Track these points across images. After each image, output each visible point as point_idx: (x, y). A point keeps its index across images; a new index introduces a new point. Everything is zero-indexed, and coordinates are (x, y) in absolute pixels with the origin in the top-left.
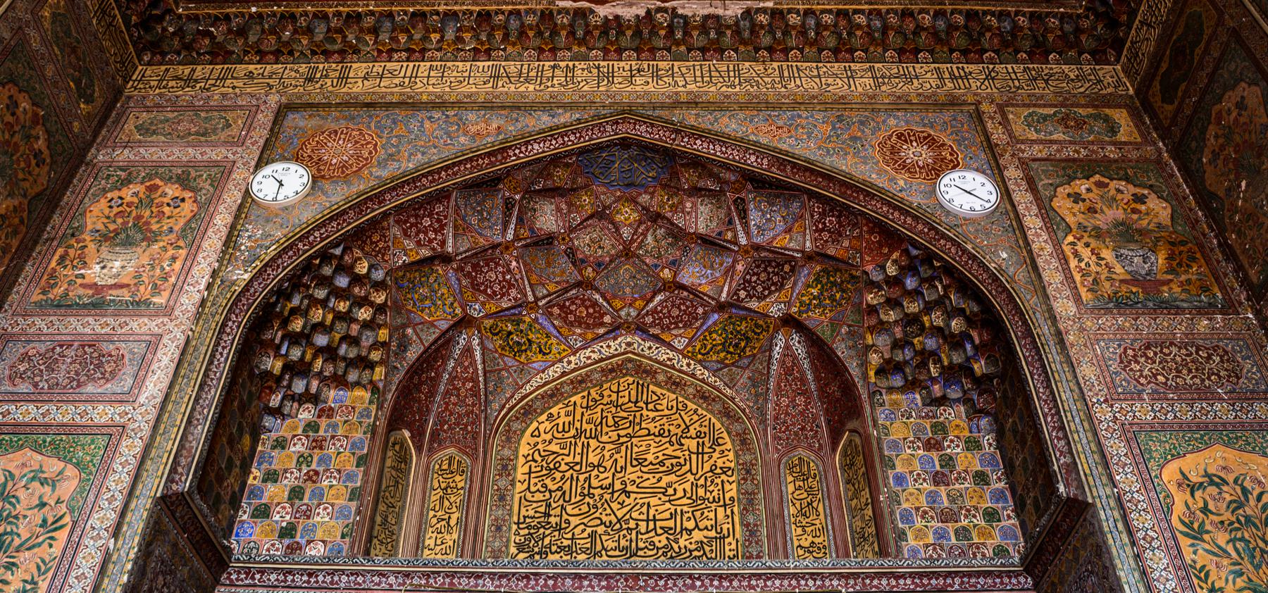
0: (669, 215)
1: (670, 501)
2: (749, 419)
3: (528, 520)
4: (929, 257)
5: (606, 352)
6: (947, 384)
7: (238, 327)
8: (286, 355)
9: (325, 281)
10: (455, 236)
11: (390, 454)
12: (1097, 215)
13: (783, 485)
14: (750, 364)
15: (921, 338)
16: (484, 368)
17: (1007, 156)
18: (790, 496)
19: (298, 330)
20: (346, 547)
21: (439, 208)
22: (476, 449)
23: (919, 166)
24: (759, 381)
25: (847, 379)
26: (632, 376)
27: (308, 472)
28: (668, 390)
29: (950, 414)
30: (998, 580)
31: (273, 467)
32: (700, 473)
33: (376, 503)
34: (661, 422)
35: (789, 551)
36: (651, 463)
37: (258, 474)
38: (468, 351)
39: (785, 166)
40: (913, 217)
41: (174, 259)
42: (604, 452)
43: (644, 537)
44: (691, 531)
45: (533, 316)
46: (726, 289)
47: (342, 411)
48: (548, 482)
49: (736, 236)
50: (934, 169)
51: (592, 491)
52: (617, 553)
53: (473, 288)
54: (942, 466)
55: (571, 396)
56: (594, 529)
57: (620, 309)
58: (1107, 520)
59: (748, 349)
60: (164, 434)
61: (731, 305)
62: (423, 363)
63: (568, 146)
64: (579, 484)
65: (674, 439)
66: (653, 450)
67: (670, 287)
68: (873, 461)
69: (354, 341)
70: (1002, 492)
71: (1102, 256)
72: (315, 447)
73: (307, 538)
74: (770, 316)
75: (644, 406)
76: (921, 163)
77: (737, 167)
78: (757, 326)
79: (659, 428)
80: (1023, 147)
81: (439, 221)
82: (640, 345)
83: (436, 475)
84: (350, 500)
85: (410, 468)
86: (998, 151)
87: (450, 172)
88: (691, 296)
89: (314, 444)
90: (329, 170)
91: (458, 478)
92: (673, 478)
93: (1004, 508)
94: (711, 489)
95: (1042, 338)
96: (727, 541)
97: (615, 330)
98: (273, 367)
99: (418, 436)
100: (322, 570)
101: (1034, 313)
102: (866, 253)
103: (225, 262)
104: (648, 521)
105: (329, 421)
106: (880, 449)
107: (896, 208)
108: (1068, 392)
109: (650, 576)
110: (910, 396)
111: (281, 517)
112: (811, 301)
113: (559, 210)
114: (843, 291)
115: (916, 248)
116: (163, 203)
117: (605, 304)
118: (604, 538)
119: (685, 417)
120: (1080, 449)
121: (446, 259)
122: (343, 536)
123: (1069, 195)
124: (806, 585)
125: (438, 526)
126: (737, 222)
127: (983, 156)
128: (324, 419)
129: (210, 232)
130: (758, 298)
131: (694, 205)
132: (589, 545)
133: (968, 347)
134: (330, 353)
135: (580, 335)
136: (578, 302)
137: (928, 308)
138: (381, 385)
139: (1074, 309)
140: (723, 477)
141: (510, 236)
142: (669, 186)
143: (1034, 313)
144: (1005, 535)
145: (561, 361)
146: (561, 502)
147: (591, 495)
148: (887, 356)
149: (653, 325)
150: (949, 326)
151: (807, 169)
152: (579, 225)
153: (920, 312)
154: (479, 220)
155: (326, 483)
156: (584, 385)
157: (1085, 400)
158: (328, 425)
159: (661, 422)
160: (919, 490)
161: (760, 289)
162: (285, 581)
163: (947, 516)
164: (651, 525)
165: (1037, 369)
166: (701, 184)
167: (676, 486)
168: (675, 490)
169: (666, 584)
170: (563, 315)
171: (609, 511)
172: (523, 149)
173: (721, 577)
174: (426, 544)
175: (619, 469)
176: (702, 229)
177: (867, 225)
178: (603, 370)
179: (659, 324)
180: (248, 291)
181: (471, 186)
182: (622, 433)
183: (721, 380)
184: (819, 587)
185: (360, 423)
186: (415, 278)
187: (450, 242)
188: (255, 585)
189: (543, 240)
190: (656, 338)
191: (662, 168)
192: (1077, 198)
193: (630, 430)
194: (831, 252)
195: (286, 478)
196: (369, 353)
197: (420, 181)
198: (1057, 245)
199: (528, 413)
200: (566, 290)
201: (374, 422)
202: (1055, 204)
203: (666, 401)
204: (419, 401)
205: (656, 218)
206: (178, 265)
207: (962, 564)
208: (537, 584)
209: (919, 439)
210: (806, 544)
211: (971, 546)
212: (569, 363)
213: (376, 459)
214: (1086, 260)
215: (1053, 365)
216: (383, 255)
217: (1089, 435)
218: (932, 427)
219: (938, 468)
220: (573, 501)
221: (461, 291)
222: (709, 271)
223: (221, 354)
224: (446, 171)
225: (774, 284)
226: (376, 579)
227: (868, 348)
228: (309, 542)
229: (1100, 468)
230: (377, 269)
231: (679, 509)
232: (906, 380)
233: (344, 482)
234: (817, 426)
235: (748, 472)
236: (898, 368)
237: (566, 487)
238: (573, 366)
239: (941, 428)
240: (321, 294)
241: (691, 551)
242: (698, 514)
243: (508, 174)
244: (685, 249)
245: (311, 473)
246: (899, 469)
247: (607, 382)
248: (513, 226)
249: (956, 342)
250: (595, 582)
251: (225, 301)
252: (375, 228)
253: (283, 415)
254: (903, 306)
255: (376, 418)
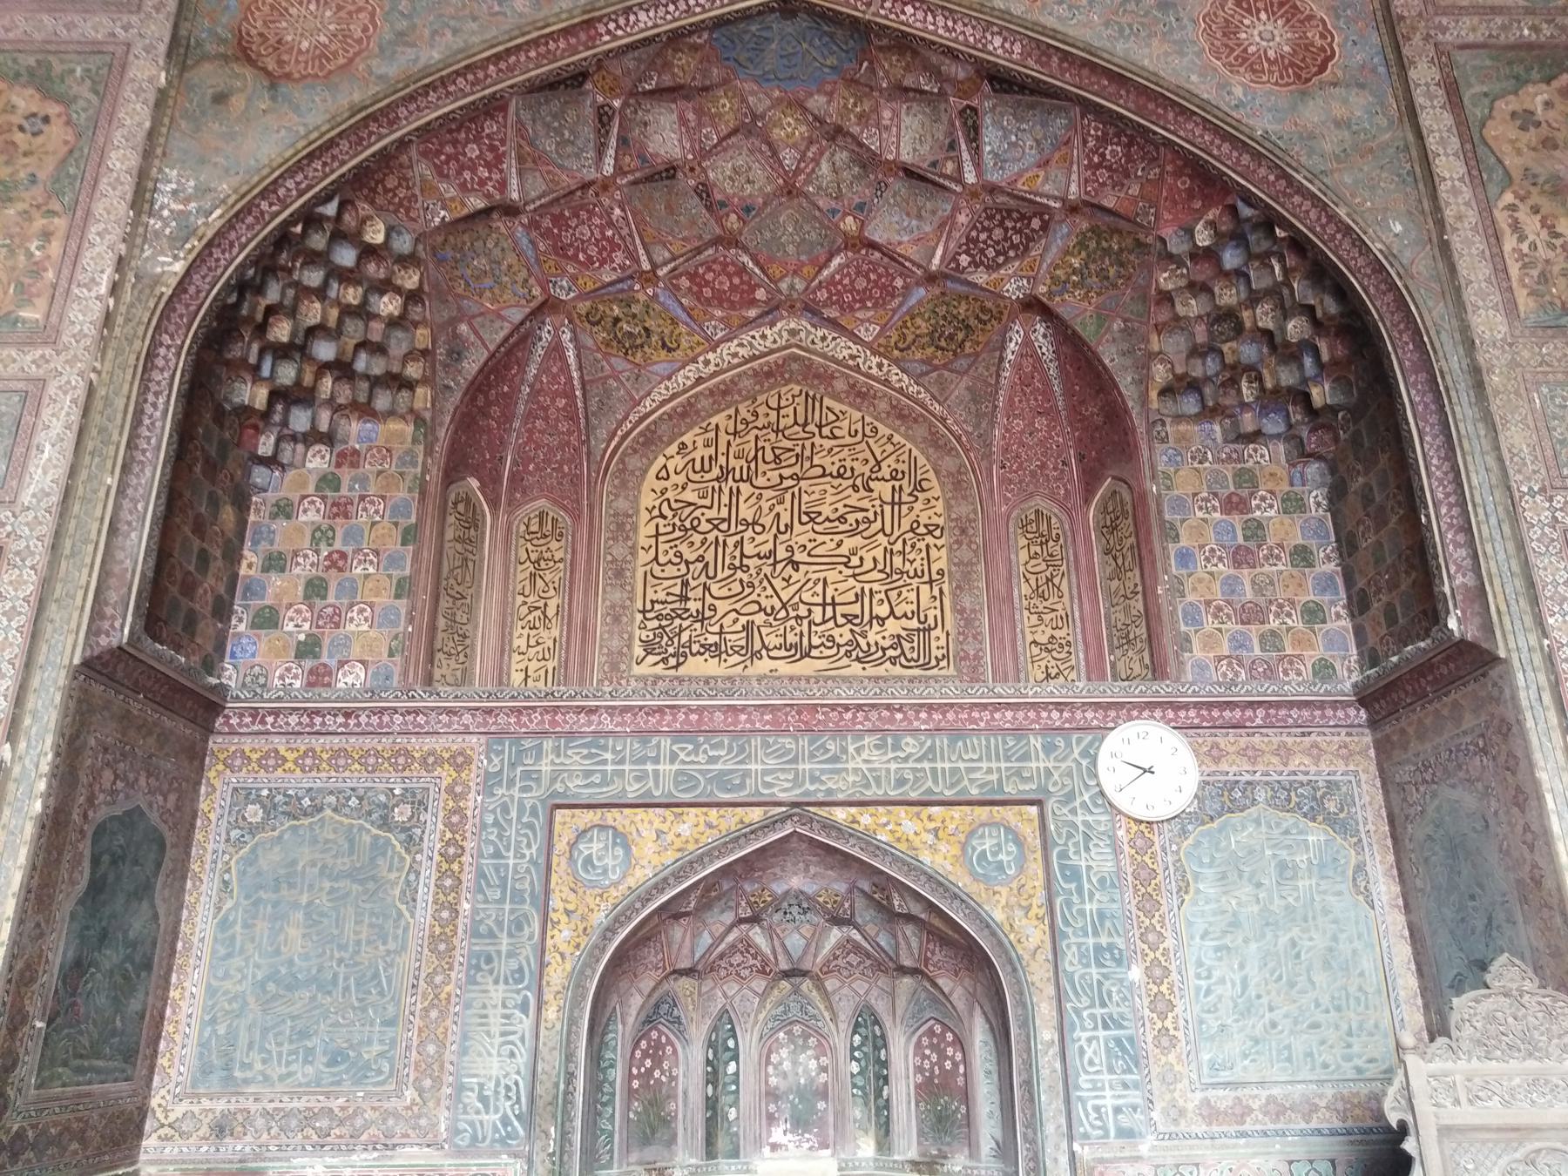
0: (855, 130)
1: (854, 576)
2: (966, 451)
3: (657, 607)
4: (1269, 222)
5: (760, 346)
6: (1264, 411)
7: (178, 355)
8: (272, 377)
9: (315, 258)
10: (520, 173)
11: (451, 519)
12: (1557, 153)
13: (1013, 550)
14: (970, 367)
15: (1234, 344)
16: (582, 377)
17: (1417, 39)
18: (1022, 569)
19: (285, 339)
20: (397, 671)
21: (490, 127)
22: (578, 501)
23: (1268, 60)
24: (982, 396)
25: (1115, 401)
26: (798, 383)
27: (330, 554)
28: (850, 405)
29: (1262, 456)
30: (1318, 713)
31: (275, 547)
32: (896, 534)
33: (436, 599)
34: (841, 456)
35: (1020, 649)
36: (827, 519)
37: (254, 559)
38: (556, 349)
39: (1049, 57)
40: (1252, 155)
41: (46, 235)
42: (762, 503)
43: (819, 629)
44: (883, 620)
45: (650, 291)
46: (939, 252)
47: (373, 456)
48: (683, 548)
49: (960, 169)
50: (1292, 64)
51: (745, 561)
52: (783, 653)
53: (557, 254)
54: (1246, 538)
55: (711, 416)
56: (750, 618)
57: (781, 278)
58: (1527, 687)
59: (968, 344)
60: (73, 555)
61: (946, 276)
62: (490, 373)
63: (695, 14)
64: (728, 551)
65: (859, 482)
66: (830, 499)
67: (854, 246)
68: (1149, 532)
69: (379, 349)
70: (1331, 578)
71: (1559, 229)
72: (336, 515)
73: (338, 657)
74: (1004, 297)
75: (816, 430)
76: (1271, 54)
77: (971, 56)
78: (983, 309)
79: (838, 464)
80: (1445, 21)
81: (492, 148)
82: (809, 333)
83: (522, 541)
84: (397, 596)
85: (484, 533)
86: (1402, 29)
87: (503, 65)
88: (886, 260)
89: (335, 510)
90: (297, 61)
91: (554, 545)
92: (857, 541)
93: (1332, 603)
94: (911, 557)
95: (1448, 377)
96: (934, 634)
97: (771, 311)
98: (253, 397)
99: (490, 483)
100: (364, 709)
101: (1438, 333)
102: (1166, 208)
103: (139, 241)
104: (824, 605)
105: (353, 472)
106: (1160, 512)
107: (1226, 137)
108: (1483, 472)
109: (833, 707)
110: (1207, 426)
111: (296, 626)
112: (1069, 276)
113: (683, 121)
114: (1122, 265)
115: (1251, 205)
116: (10, 124)
117: (757, 270)
118: (764, 631)
119: (874, 447)
120: (1494, 570)
121: (511, 211)
122: (391, 655)
123: (1514, 115)
124: (1049, 718)
125: (530, 617)
126: (963, 147)
127: (1375, 39)
128: (345, 469)
129: (103, 185)
130: (988, 267)
131: (896, 114)
132: (743, 643)
133: (1308, 361)
134: (342, 369)
135: (721, 320)
136: (716, 267)
137: (1253, 299)
138: (427, 415)
139: (1504, 329)
140: (929, 539)
141: (608, 168)
142: (857, 82)
143: (1438, 333)
144: (1330, 644)
145: (695, 361)
146: (703, 578)
147: (744, 568)
148: (1179, 370)
149: (828, 303)
150: (1283, 330)
151: (1085, 63)
152: (715, 146)
153: (1240, 304)
154: (558, 144)
155: (358, 571)
156: (728, 398)
157: (1509, 488)
158: (354, 480)
159: (841, 456)
160: (1211, 574)
161: (991, 253)
162: (312, 725)
163: (1251, 614)
164: (829, 609)
165: (1432, 426)
166: (908, 82)
167: (861, 553)
168: (861, 559)
169: (855, 717)
170: (695, 289)
171: (770, 591)
172: (622, 21)
173: (930, 708)
174: (515, 646)
175: (782, 529)
176: (906, 157)
177: (1173, 161)
178: (756, 374)
179: (837, 302)
180: (185, 291)
181: (540, 89)
182: (786, 472)
183: (927, 390)
184: (1067, 721)
185: (401, 474)
186: (464, 243)
187: (514, 182)
188: (268, 733)
189: (660, 173)
190: (833, 324)
191: (847, 52)
192: (1526, 119)
193: (797, 469)
194: (1110, 202)
195: (298, 564)
196: (404, 366)
197: (454, 83)
198: (1486, 210)
199: (650, 441)
200: (699, 250)
201: (423, 474)
202: (1491, 132)
203: (845, 424)
204: (490, 430)
205: (837, 133)
206: (55, 248)
207: (1267, 691)
208: (675, 720)
209: (1215, 495)
210: (1043, 639)
211: (1281, 659)
212: (707, 363)
213: (429, 531)
214: (1531, 237)
215: (1461, 426)
216: (408, 210)
217: (1511, 546)
218: (1235, 476)
219: (1240, 540)
220: (720, 576)
221: (537, 260)
222: (914, 223)
223: (154, 405)
224: (496, 64)
225: (1013, 246)
226: (444, 718)
227: (1151, 356)
228: (342, 664)
229: (1522, 602)
230: (399, 233)
231: (867, 587)
232: (1204, 406)
233: (386, 569)
234: (1064, 463)
235: (963, 531)
236: (1194, 386)
237: (709, 556)
238: (712, 368)
239: (1247, 478)
240: (314, 278)
241: (884, 650)
242: (893, 594)
243: (599, 64)
244: (880, 187)
245: (335, 556)
246: (1184, 543)
247: (762, 392)
248: (611, 152)
249: (1288, 353)
250: (756, 715)
251: (148, 314)
252: (388, 167)
253: (283, 466)
254: (1213, 295)
255: (425, 470)
